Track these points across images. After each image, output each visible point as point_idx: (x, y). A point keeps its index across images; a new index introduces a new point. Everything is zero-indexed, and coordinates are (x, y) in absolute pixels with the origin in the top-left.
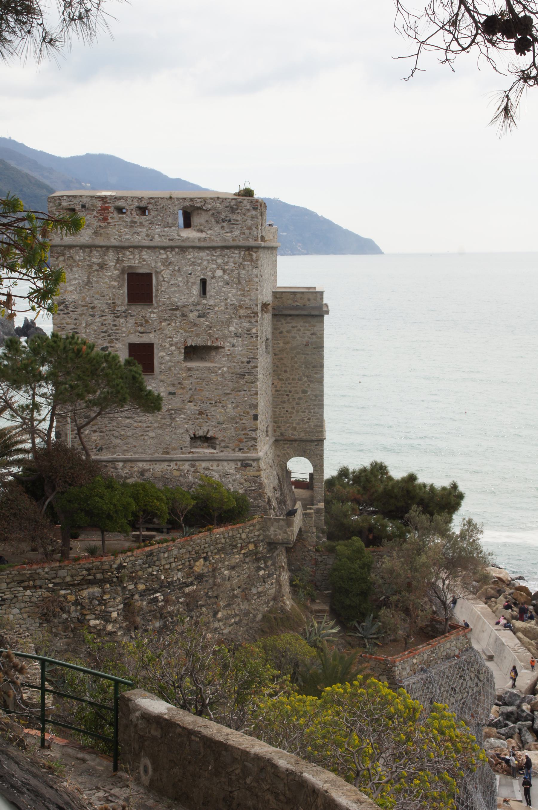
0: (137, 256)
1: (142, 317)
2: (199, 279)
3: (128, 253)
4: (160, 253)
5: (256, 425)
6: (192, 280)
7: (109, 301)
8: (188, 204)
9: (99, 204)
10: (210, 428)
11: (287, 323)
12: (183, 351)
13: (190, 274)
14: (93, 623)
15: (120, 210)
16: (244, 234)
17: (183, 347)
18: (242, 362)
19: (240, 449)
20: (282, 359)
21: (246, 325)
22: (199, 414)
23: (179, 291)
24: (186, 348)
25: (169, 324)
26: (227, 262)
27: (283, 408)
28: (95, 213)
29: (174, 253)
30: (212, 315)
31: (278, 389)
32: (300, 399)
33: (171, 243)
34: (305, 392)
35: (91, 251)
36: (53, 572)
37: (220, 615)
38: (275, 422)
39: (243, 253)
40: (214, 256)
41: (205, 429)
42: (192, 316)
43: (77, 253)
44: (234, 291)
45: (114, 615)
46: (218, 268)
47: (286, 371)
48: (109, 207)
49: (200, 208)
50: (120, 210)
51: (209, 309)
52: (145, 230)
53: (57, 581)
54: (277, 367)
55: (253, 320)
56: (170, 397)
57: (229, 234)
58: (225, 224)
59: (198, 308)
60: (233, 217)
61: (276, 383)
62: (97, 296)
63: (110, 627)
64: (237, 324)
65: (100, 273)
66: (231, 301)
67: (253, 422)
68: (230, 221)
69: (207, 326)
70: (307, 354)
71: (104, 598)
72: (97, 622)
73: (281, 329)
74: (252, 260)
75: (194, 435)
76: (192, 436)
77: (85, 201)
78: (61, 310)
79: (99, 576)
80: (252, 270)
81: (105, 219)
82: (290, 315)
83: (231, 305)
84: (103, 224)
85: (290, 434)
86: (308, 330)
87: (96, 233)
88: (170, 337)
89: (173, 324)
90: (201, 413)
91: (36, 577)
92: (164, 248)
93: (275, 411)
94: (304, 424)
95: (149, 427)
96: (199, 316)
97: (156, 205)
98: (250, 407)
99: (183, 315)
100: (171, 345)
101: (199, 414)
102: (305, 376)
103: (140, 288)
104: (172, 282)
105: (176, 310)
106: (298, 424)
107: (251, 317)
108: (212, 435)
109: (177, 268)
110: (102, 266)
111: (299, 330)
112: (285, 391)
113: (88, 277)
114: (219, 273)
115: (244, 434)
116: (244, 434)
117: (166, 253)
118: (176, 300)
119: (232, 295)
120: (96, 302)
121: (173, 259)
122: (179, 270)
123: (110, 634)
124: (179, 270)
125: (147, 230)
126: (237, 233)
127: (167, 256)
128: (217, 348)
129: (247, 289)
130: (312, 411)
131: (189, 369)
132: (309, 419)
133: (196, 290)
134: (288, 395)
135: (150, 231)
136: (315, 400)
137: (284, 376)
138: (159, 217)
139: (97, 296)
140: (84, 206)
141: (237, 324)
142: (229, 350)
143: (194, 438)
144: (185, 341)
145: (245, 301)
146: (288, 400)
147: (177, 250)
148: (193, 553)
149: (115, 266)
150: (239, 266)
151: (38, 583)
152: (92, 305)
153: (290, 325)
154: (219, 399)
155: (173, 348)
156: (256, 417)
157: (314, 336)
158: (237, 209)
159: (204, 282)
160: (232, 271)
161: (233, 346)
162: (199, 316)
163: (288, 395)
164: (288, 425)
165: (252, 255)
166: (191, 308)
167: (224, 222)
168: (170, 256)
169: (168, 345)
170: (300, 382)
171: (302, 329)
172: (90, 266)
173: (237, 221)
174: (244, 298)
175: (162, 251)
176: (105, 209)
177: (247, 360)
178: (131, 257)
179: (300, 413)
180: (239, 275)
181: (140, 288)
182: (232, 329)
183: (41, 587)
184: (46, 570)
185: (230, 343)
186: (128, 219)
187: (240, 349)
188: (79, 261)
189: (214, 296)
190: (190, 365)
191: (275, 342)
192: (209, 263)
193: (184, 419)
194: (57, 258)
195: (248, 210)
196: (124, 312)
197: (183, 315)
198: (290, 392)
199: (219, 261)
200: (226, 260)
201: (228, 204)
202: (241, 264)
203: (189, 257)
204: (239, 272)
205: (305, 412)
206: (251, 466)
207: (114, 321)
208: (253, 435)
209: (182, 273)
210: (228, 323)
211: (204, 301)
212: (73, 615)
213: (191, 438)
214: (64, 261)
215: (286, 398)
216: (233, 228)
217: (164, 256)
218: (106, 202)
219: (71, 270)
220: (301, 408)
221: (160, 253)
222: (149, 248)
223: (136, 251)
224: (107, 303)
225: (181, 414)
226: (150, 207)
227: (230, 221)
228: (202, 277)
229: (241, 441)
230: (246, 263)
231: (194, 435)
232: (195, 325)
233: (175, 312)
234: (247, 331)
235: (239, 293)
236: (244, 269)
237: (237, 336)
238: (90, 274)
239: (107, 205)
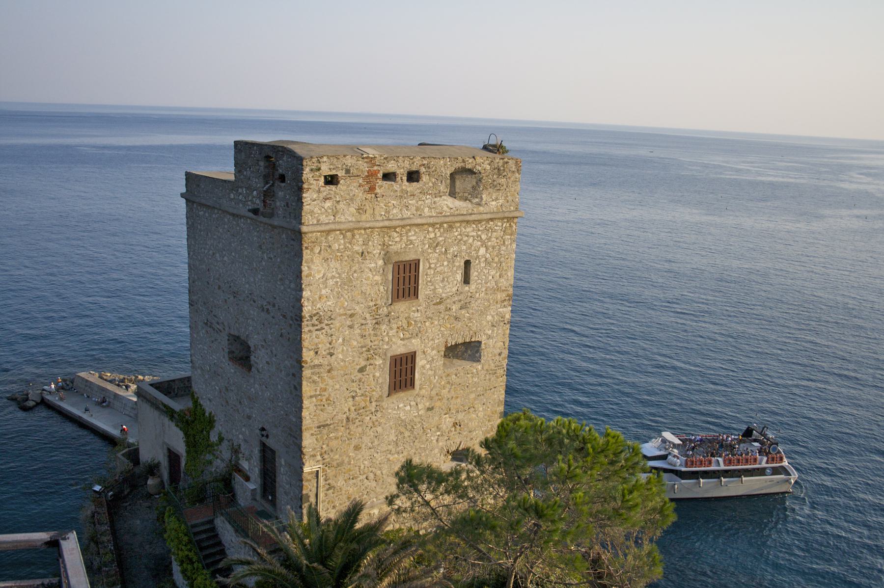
0: (405, 238)
28: (361, 181)
30: (474, 305)
41: (458, 441)
43: (336, 240)
50: (388, 176)
56: (429, 413)
59: (462, 297)
65: (363, 266)
78: (313, 325)
81: (372, 189)
87: (360, 210)
90: (455, 424)
92: (433, 225)
96: (461, 308)
97: (429, 168)
103: (406, 280)
104: (438, 269)
105: (440, 303)
114: (482, 251)
133: (459, 277)
135: (420, 203)
159: (467, 263)
162: (461, 308)
168: (438, 235)
175: (431, 229)
176: (371, 175)
181: (406, 280)
182: (489, 318)
203: (456, 234)
217: (432, 236)
218: (374, 165)
222: (417, 225)
226: (423, 170)
232: (456, 318)
239: (376, 168)
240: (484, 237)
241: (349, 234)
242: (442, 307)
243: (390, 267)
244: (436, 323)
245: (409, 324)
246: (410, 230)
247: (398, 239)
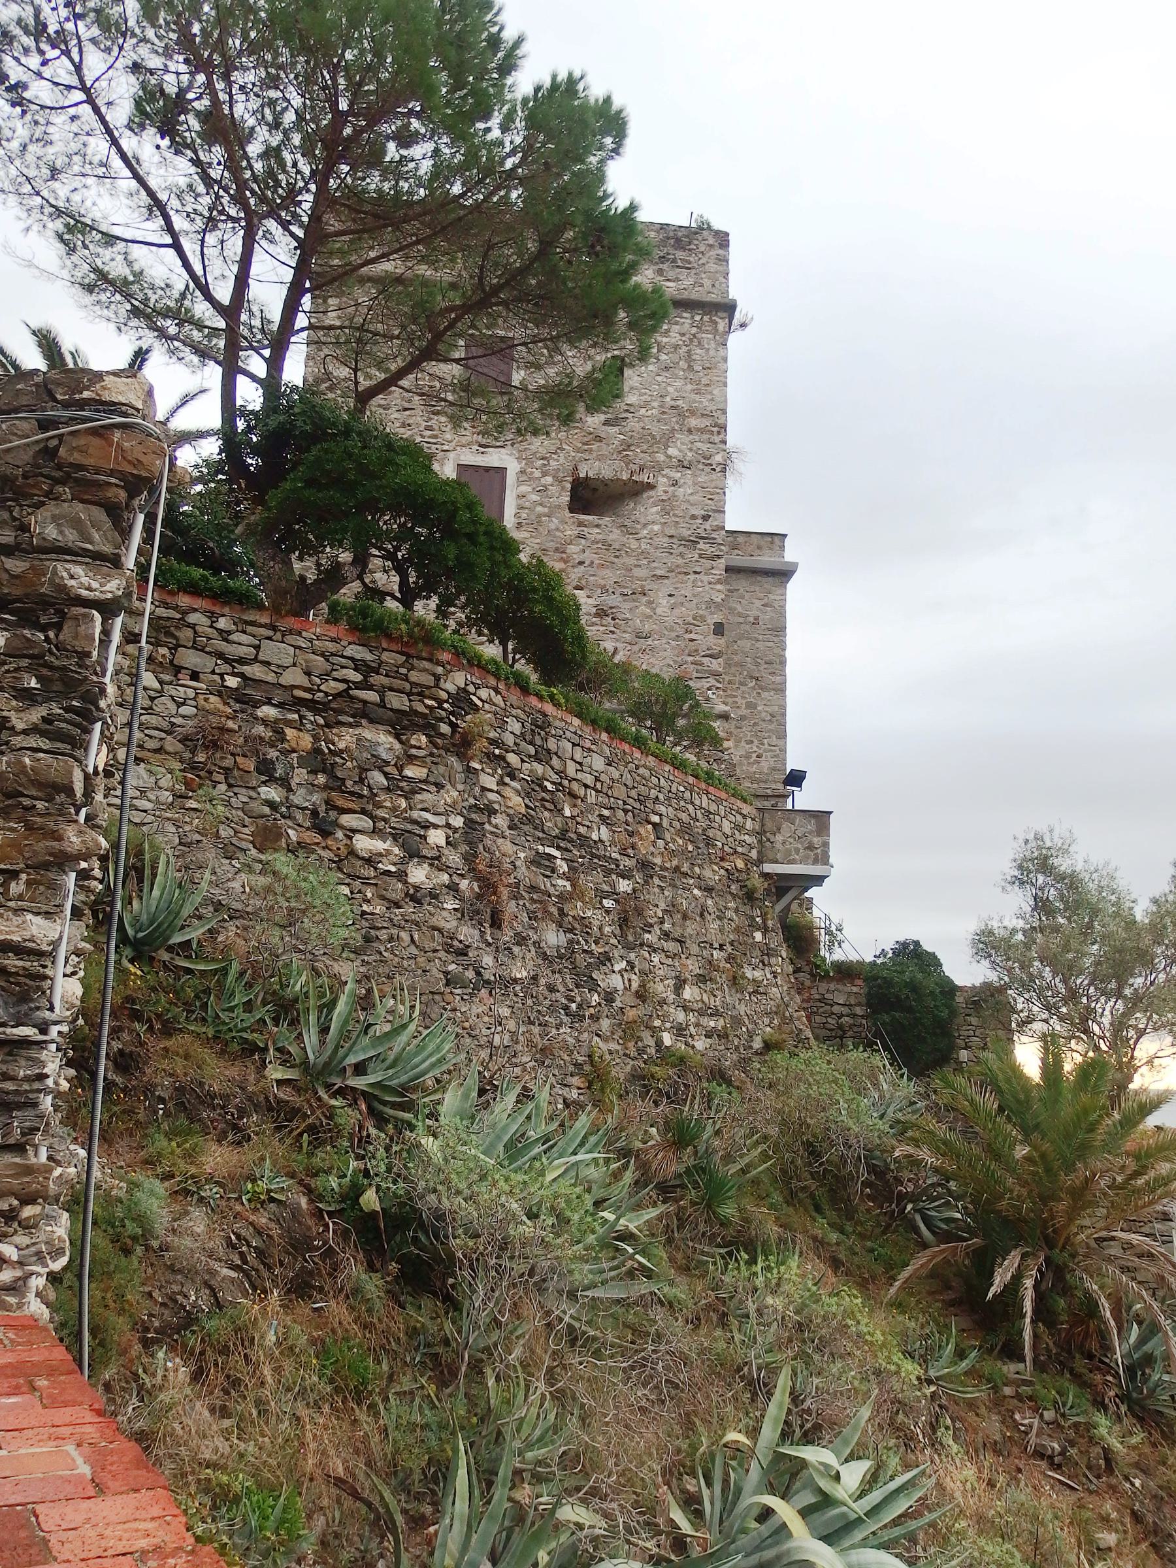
10: (618, 645)
12: (569, 486)
14: (364, 844)
16: (702, 285)
17: (570, 479)
18: (693, 517)
22: (597, 615)
30: (633, 424)
32: (743, 718)
34: (751, 706)
36: (244, 638)
37: (688, 993)
39: (698, 318)
45: (437, 837)
53: (254, 671)
55: (717, 439)
58: (665, 266)
60: (680, 254)
63: (418, 874)
69: (622, 442)
71: (408, 772)
72: (379, 845)
79: (397, 701)
91: (186, 634)
100: (545, 474)
101: (597, 615)
102: (752, 677)
123: (415, 896)
129: (704, 381)
131: (581, 524)
144: (576, 468)
148: (633, 793)
151: (190, 658)
155: (549, 479)
160: (676, 347)
161: (675, 484)
169: (537, 474)
171: (747, 595)
179: (743, 744)
182: (671, 451)
183: (195, 676)
184: (222, 623)
195: (711, 246)
210: (667, 440)
212: (298, 798)
227: (674, 261)
232: (599, 439)
237: (682, 465)
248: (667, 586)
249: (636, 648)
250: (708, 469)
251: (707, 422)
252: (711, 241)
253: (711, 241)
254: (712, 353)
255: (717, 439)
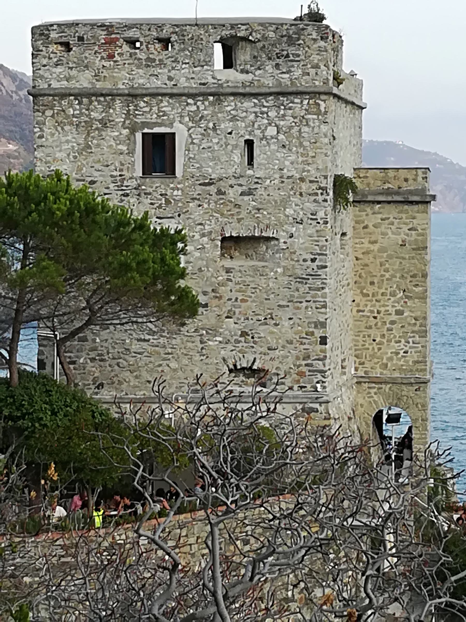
0: (155, 109)
1: (161, 195)
2: (242, 140)
3: (142, 104)
4: (188, 104)
5: (324, 351)
6: (233, 142)
7: (115, 173)
8: (226, 33)
9: (102, 35)
11: (374, 213)
13: (230, 133)
15: (132, 42)
16: (308, 74)
17: (220, 238)
18: (305, 260)
19: (301, 387)
20: (367, 265)
21: (310, 206)
22: (241, 336)
23: (213, 159)
24: (224, 239)
25: (199, 206)
26: (284, 116)
27: (369, 336)
28: (96, 48)
29: (207, 103)
30: (261, 191)
31: (361, 308)
32: (393, 323)
33: (203, 89)
35: (91, 102)
38: (356, 356)
40: (264, 107)
42: (232, 194)
43: (71, 105)
44: (293, 157)
46: (270, 124)
47: (372, 283)
48: (118, 39)
49: (245, 39)
51: (257, 183)
52: (166, 71)
54: (360, 277)
57: (287, 76)
58: (280, 61)
59: (241, 181)
60: (292, 50)
61: (358, 300)
62: (97, 166)
64: (296, 205)
65: (103, 133)
66: (288, 170)
67: (319, 347)
68: (287, 56)
69: (254, 208)
70: (404, 258)
73: (366, 223)
74: (318, 113)
75: (235, 366)
76: (231, 367)
77: (81, 31)
80: (319, 126)
81: (111, 57)
82: (379, 202)
83: (288, 177)
84: (107, 64)
85: (377, 372)
86: (405, 224)
88: (201, 224)
89: (206, 206)
90: (244, 334)
93: (358, 341)
94: (399, 360)
95: (169, 354)
97: (183, 35)
98: (316, 327)
99: (220, 192)
100: (203, 235)
101: (241, 336)
103: (159, 153)
105: (210, 184)
106: (390, 359)
107: (316, 194)
108: (260, 366)
109: (211, 125)
110: (105, 123)
111: (392, 224)
112: (372, 312)
113: (85, 139)
115: (307, 365)
116: (307, 365)
117: (195, 104)
118: (210, 170)
119: (290, 162)
120: (96, 174)
121: (205, 112)
122: (214, 129)
124: (214, 129)
125: (169, 71)
126: (298, 73)
127: (198, 107)
128: (268, 239)
129: (311, 154)
130: (411, 340)
131: (228, 271)
132: (406, 352)
133: (238, 156)
134: (375, 318)
136: (415, 324)
137: (370, 290)
138: (187, 52)
139: (97, 166)
140: (81, 39)
141: (296, 205)
142: (285, 243)
143: (234, 370)
145: (308, 171)
146: (376, 325)
147: (211, 98)
149: (124, 122)
150: (301, 121)
152: (89, 179)
153: (380, 216)
154: (271, 314)
155: (205, 239)
156: (323, 341)
157: (413, 232)
158: (298, 39)
159: (250, 144)
160: (291, 128)
163: (375, 318)
164: (376, 360)
165: (319, 105)
166: (232, 182)
167: (278, 58)
168: (202, 108)
169: (197, 236)
170: (393, 299)
171: (396, 221)
172: (89, 124)
173: (298, 56)
174: (307, 168)
175: (190, 101)
176: (110, 42)
177: (313, 257)
178: (147, 109)
179: (393, 343)
180: (300, 135)
181: (159, 153)
182: (289, 211)
185: (287, 233)
186: (143, 56)
187: (301, 241)
188: (73, 116)
189: (264, 165)
190: (228, 263)
191: (357, 241)
192: (257, 116)
193: (220, 342)
194: (43, 113)
195: (315, 40)
196: (135, 188)
197: (220, 192)
198: (379, 312)
199: (272, 114)
200: (282, 112)
201: (284, 33)
202: (303, 117)
203: (229, 108)
204: (300, 130)
205: (400, 342)
206: (317, 411)
207: (122, 201)
208: (319, 365)
209: (219, 132)
210: (284, 203)
211: (250, 172)
213: (231, 371)
214: (53, 116)
215: (372, 322)
216: (293, 66)
217: (194, 108)
219: (62, 129)
220: (395, 337)
221: (188, 104)
222: (172, 96)
223: (154, 101)
224: (112, 176)
225: (216, 336)
226: (174, 38)
227: (287, 56)
228: (247, 137)
229: (301, 374)
230: (310, 116)
231: (235, 366)
233: (208, 188)
234: (312, 214)
235: (300, 159)
236: (307, 125)
238: (88, 134)
239: (113, 36)
240: (272, 114)
241: (85, 100)
242: (213, 189)
243: (139, 137)
244: (206, 206)
245: (168, 202)
246: (162, 101)
247: (147, 109)
248: (289, 312)
249: (268, 358)
250: (314, 223)
251: (314, 186)
252: (314, 35)
253: (314, 35)
254: (316, 130)
255: (320, 198)
